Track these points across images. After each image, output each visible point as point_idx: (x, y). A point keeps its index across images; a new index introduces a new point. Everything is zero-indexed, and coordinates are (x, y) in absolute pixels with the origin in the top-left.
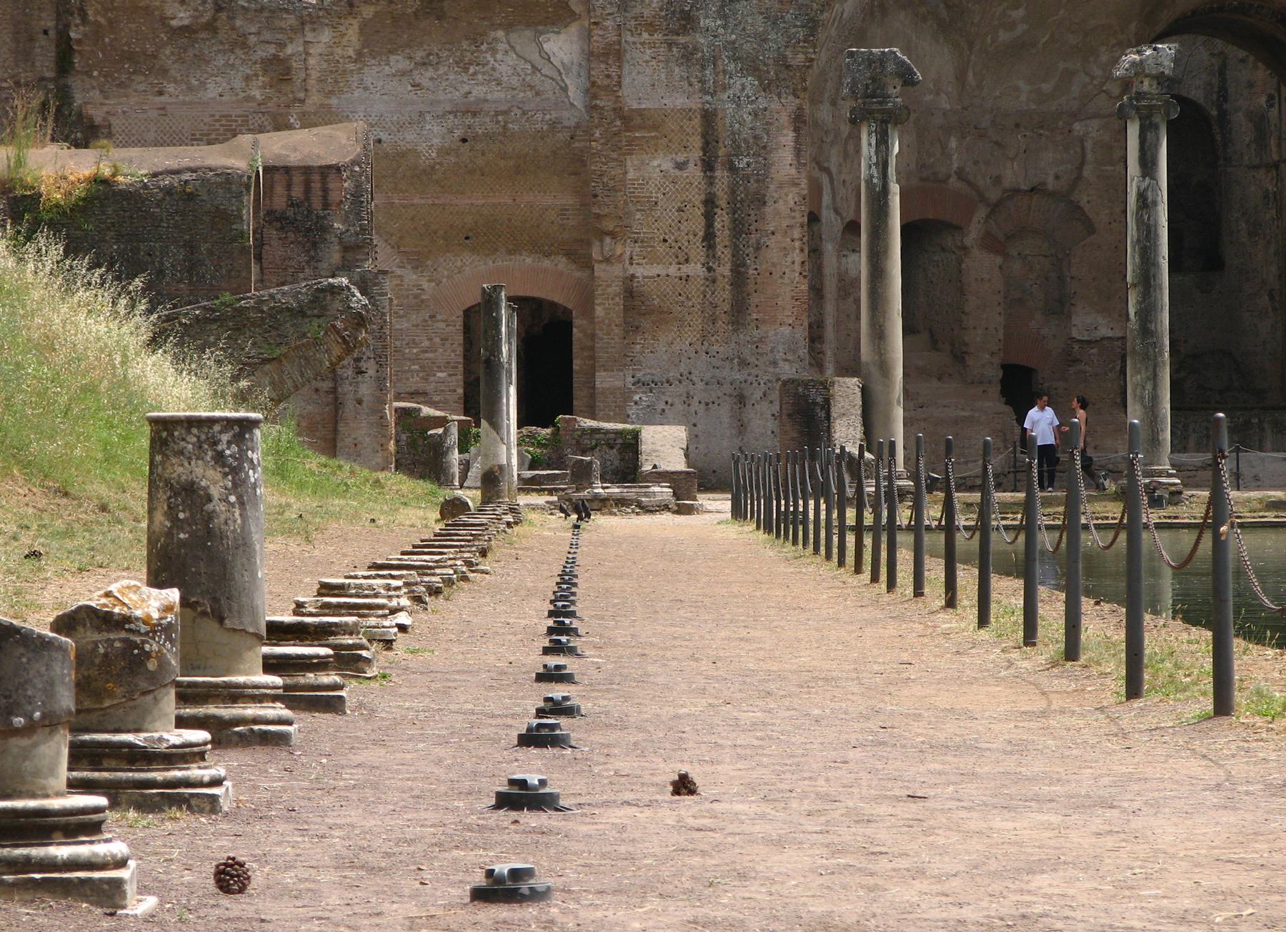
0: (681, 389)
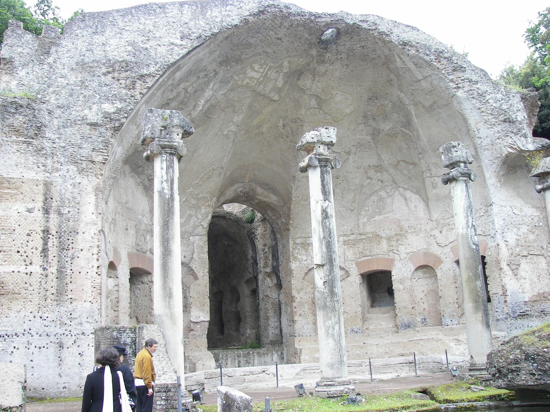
0: (24, 339)
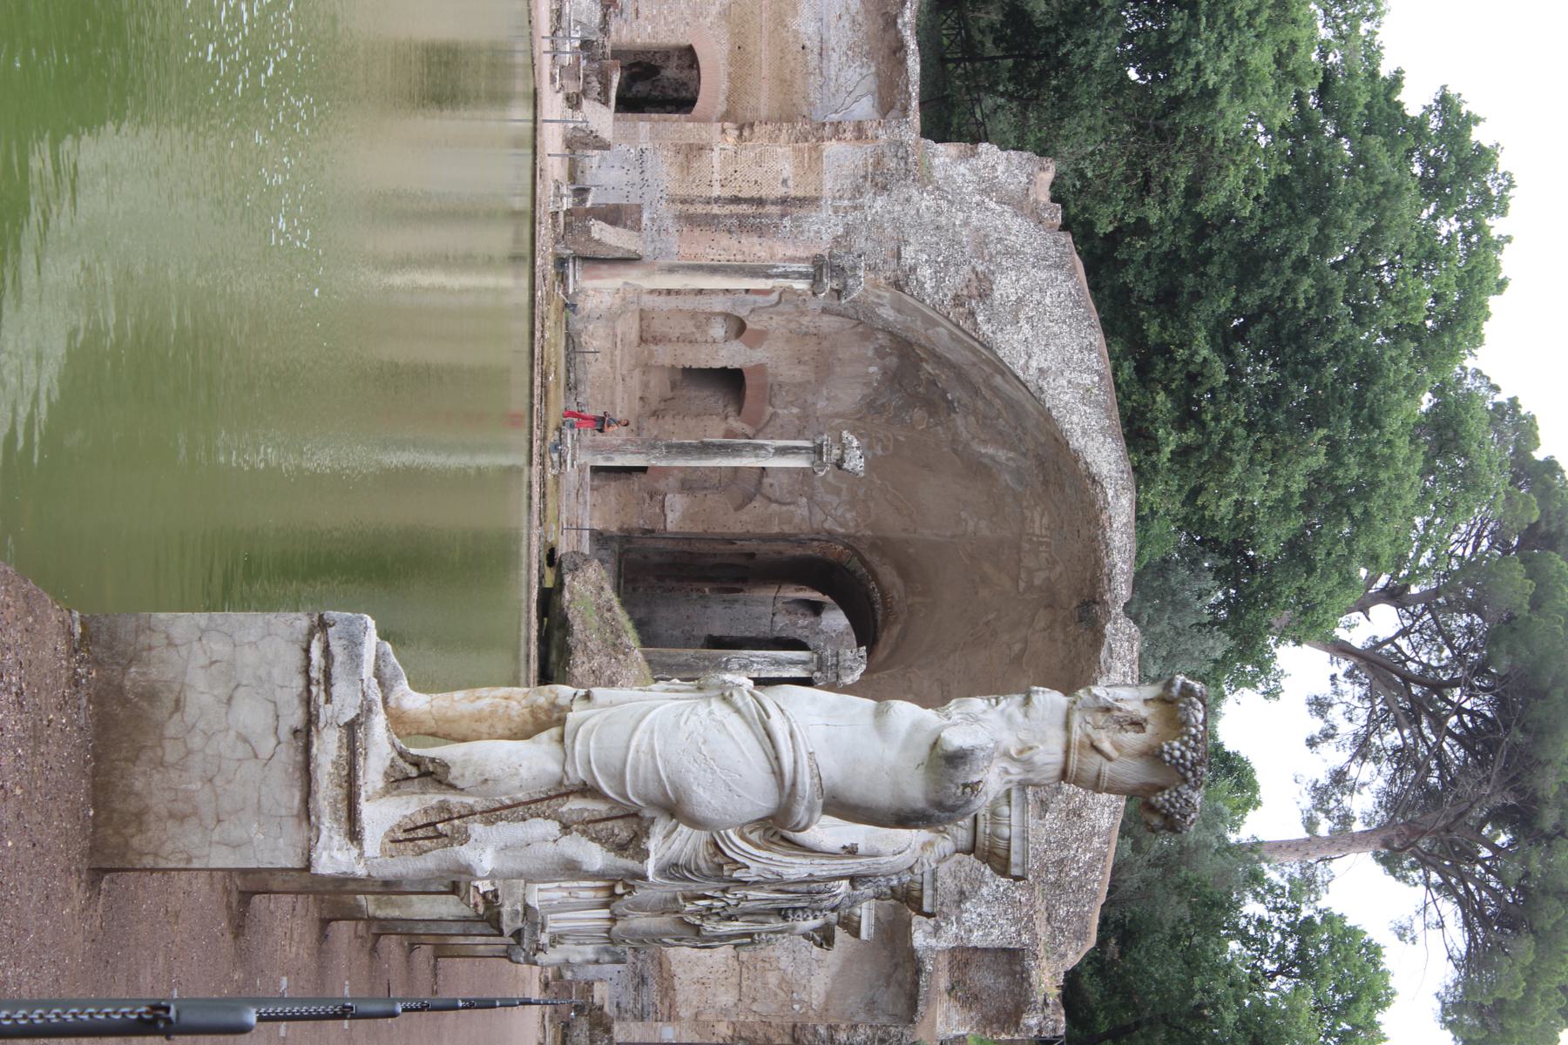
0: (637, 179)
